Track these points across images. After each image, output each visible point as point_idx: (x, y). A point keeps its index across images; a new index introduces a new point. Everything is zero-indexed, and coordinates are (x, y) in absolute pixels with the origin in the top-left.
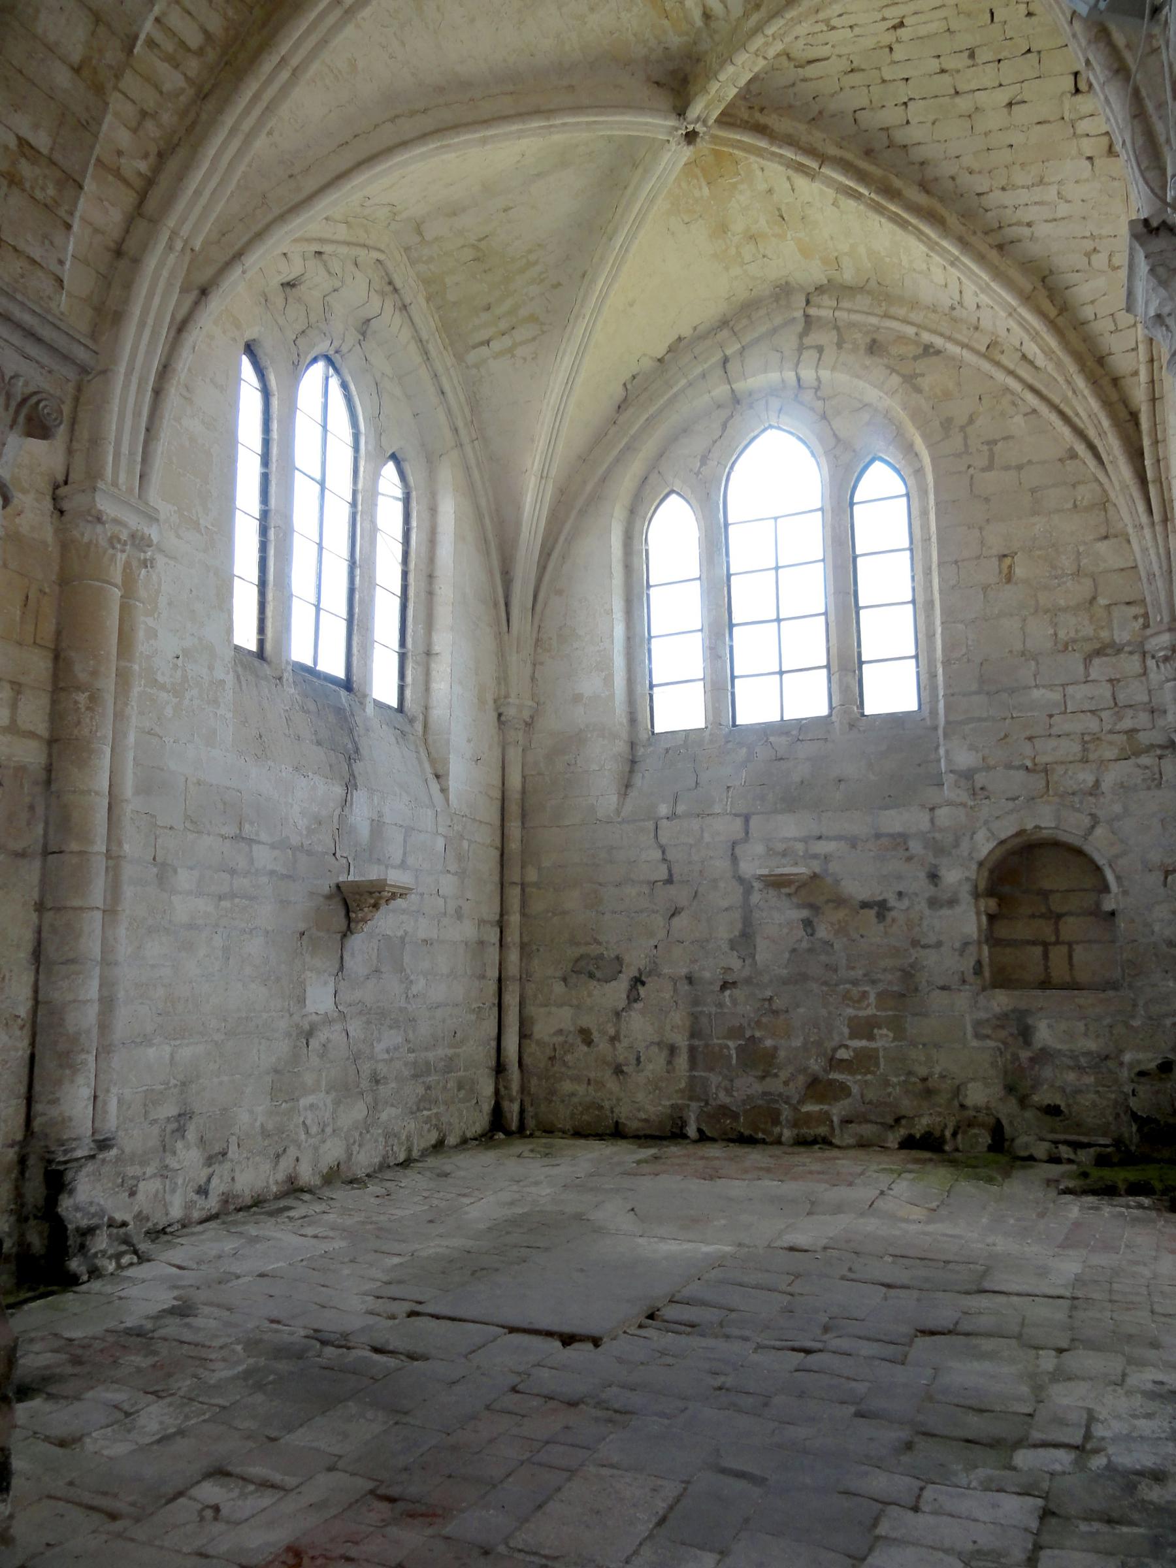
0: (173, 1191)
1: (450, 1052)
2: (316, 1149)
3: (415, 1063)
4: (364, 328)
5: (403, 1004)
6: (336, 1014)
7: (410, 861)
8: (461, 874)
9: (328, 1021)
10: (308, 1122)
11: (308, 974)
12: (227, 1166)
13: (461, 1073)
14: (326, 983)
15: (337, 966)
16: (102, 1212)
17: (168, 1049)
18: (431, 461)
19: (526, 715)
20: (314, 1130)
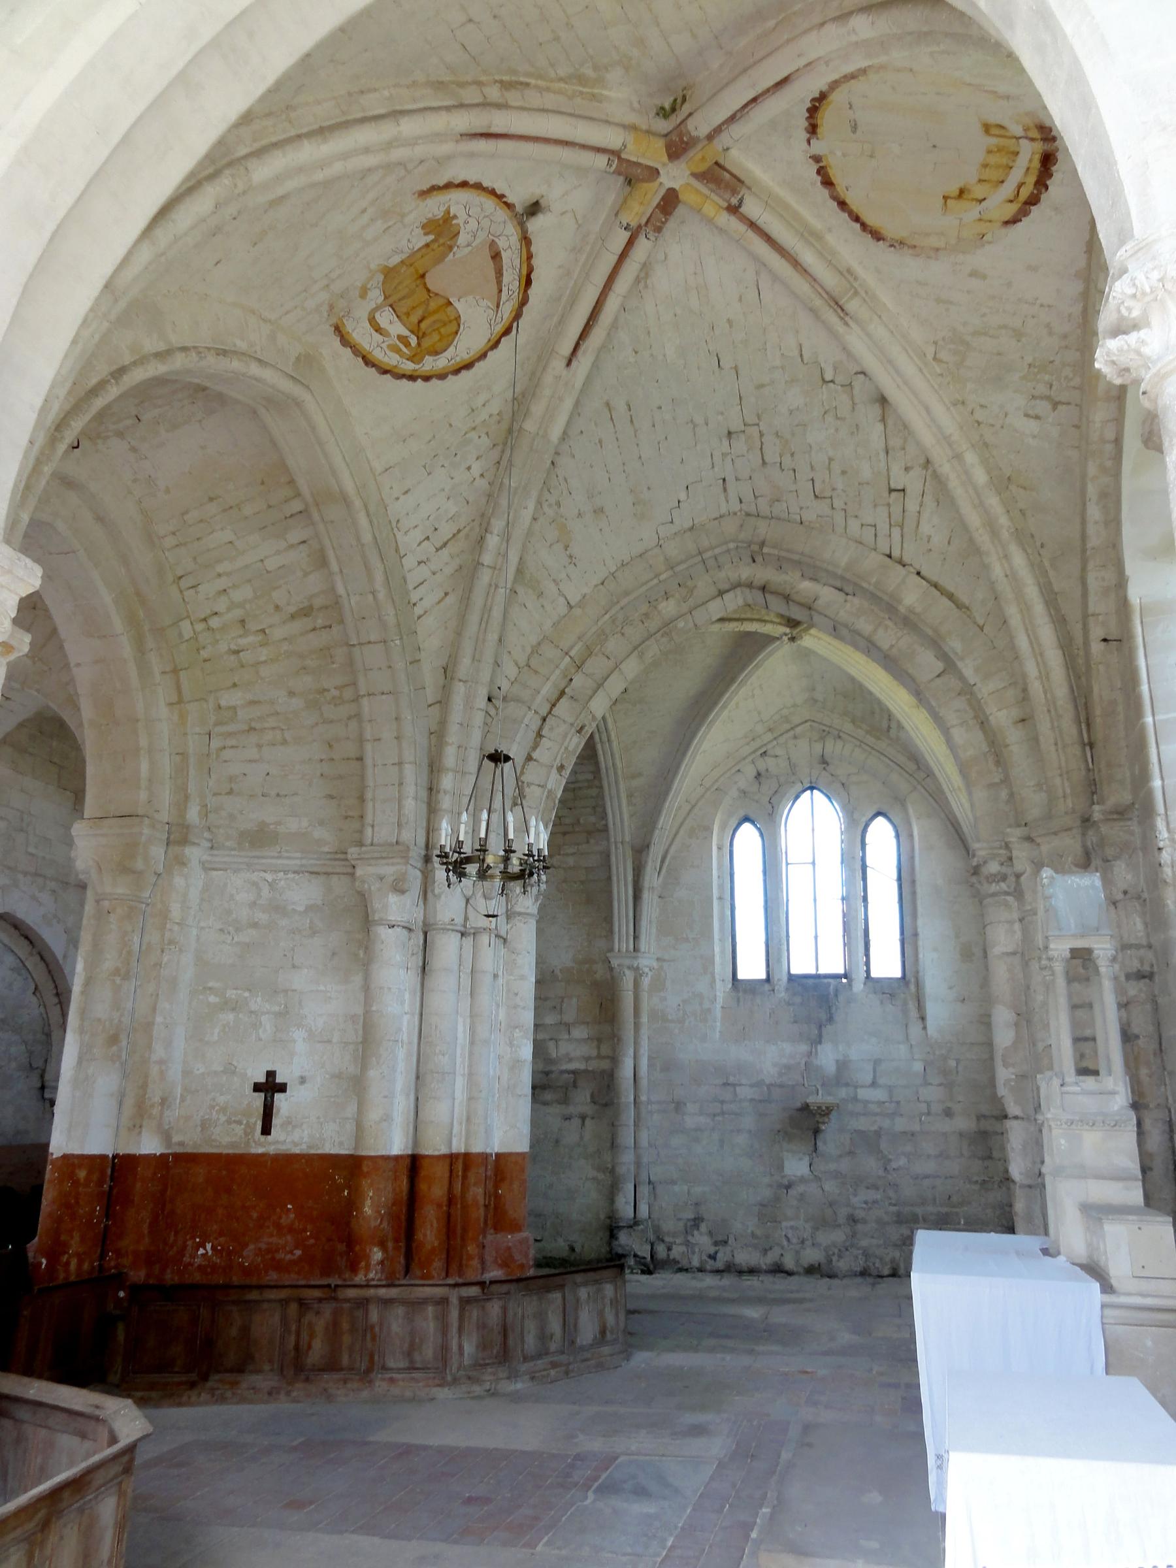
0: (693, 1253)
1: (945, 1210)
2: (797, 1252)
3: (898, 1214)
4: (824, 761)
6: (812, 1177)
7: (881, 1081)
9: (802, 1180)
10: (790, 1236)
11: (785, 1153)
12: (728, 1249)
14: (801, 1159)
15: (812, 1149)
16: (632, 1249)
17: (685, 1188)
20: (795, 1241)
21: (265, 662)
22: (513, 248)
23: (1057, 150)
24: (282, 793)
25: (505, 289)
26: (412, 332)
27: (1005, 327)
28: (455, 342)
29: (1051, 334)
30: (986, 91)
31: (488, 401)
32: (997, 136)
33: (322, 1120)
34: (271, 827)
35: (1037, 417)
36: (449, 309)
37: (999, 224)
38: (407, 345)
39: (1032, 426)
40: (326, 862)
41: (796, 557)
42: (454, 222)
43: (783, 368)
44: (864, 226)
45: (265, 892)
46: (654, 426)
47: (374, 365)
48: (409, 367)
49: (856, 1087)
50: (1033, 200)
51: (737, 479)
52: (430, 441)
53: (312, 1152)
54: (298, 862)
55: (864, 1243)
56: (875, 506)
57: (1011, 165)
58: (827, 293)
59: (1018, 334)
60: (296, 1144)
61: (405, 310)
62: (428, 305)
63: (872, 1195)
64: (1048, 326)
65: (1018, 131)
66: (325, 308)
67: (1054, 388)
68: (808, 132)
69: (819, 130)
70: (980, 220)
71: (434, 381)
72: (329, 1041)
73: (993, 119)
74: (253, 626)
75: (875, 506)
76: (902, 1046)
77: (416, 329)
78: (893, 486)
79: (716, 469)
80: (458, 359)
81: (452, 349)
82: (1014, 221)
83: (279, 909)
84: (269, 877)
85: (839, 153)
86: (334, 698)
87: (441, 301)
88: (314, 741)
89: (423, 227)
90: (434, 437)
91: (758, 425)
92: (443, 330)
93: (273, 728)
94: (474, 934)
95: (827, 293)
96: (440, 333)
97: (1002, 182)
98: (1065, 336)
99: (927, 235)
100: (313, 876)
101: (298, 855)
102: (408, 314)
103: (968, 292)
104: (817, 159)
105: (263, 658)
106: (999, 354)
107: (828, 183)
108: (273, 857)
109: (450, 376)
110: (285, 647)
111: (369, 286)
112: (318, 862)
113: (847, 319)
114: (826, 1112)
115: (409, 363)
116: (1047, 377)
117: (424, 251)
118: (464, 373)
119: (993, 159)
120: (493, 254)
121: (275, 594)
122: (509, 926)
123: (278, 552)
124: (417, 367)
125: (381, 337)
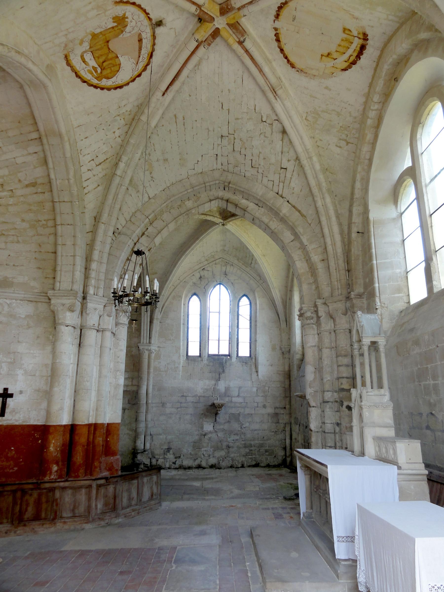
0: (167, 462)
1: (261, 442)
2: (207, 460)
3: (245, 444)
4: (226, 274)
5: (239, 429)
7: (241, 395)
8: (265, 397)
9: (210, 432)
10: (204, 454)
11: (205, 422)
12: (181, 460)
13: (267, 448)
14: (210, 424)
16: (143, 461)
17: (165, 436)
18: (254, 292)
19: (287, 349)
20: (206, 455)
21: (11, 205)
22: (148, 39)
23: (367, 44)
24: (16, 265)
25: (141, 56)
26: (99, 66)
27: (334, 110)
28: (116, 75)
29: (350, 116)
30: (350, 14)
31: (126, 104)
32: (348, 34)
33: (30, 410)
34: (10, 279)
35: (340, 147)
36: (117, 59)
37: (340, 70)
38: (96, 72)
39: (338, 150)
40: (37, 297)
41: (242, 190)
42: (126, 20)
43: (247, 113)
44: (288, 61)
45: (6, 308)
46: (193, 128)
47: (80, 78)
48: (95, 82)
49: (232, 397)
50: (354, 63)
51: (222, 156)
52: (99, 117)
53: (24, 424)
54: (23, 296)
55: (232, 455)
56: (275, 173)
57: (349, 47)
58: (271, 85)
59: (338, 114)
60: (17, 421)
61: (97, 55)
62: (108, 56)
63: (236, 437)
64: (350, 113)
65: (355, 34)
66: (63, 45)
67: (348, 137)
68: (275, 17)
69: (280, 17)
70: (333, 67)
71: (105, 90)
72: (34, 375)
73: (348, 27)
74: (7, 188)
75: (275, 173)
76: (249, 382)
77: (101, 65)
78: (282, 167)
79: (214, 150)
80: (117, 83)
81: (115, 78)
82: (345, 70)
83: (12, 316)
84: (8, 301)
85: (285, 29)
86: (43, 225)
87: (114, 55)
88: (33, 243)
89: (114, 18)
90: (101, 115)
91: (234, 134)
92: (112, 68)
93: (13, 235)
94: (102, 331)
95: (271, 85)
96: (111, 69)
97: (344, 53)
98: (355, 118)
99: (312, 69)
100: (30, 302)
101: (23, 292)
102: (98, 58)
103: (323, 95)
104: (276, 29)
105: (11, 203)
106: (330, 121)
107: (278, 40)
108: (10, 293)
109: (112, 90)
110: (22, 199)
111: (84, 40)
112: (33, 296)
113: (277, 97)
114: (221, 406)
115: (95, 80)
116: (346, 132)
117: (111, 30)
118: (118, 89)
119: (343, 44)
120: (139, 39)
121: (19, 175)
122: (117, 328)
123: (23, 156)
124: (99, 82)
125: (85, 65)
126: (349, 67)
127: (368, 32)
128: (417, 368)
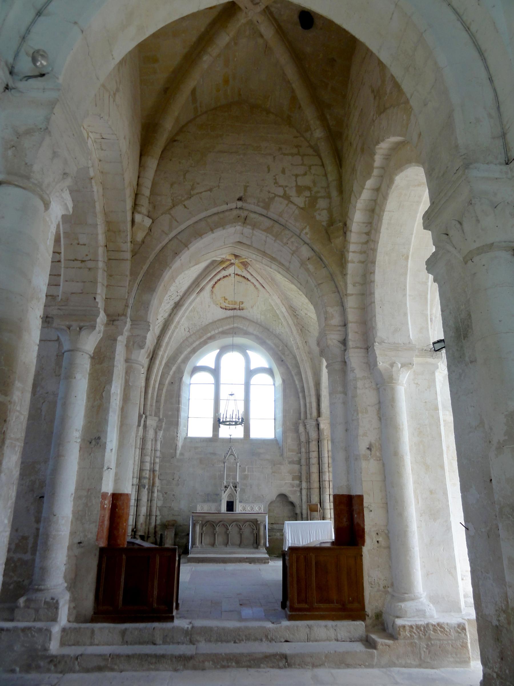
35: (185, 330)
43: (180, 284)
44: (215, 284)
50: (226, 309)
65: (241, 306)
82: (221, 308)
98: (202, 325)
99: (216, 296)
104: (230, 275)
106: (195, 317)
126: (223, 309)
127: (244, 311)
128: (219, 473)
